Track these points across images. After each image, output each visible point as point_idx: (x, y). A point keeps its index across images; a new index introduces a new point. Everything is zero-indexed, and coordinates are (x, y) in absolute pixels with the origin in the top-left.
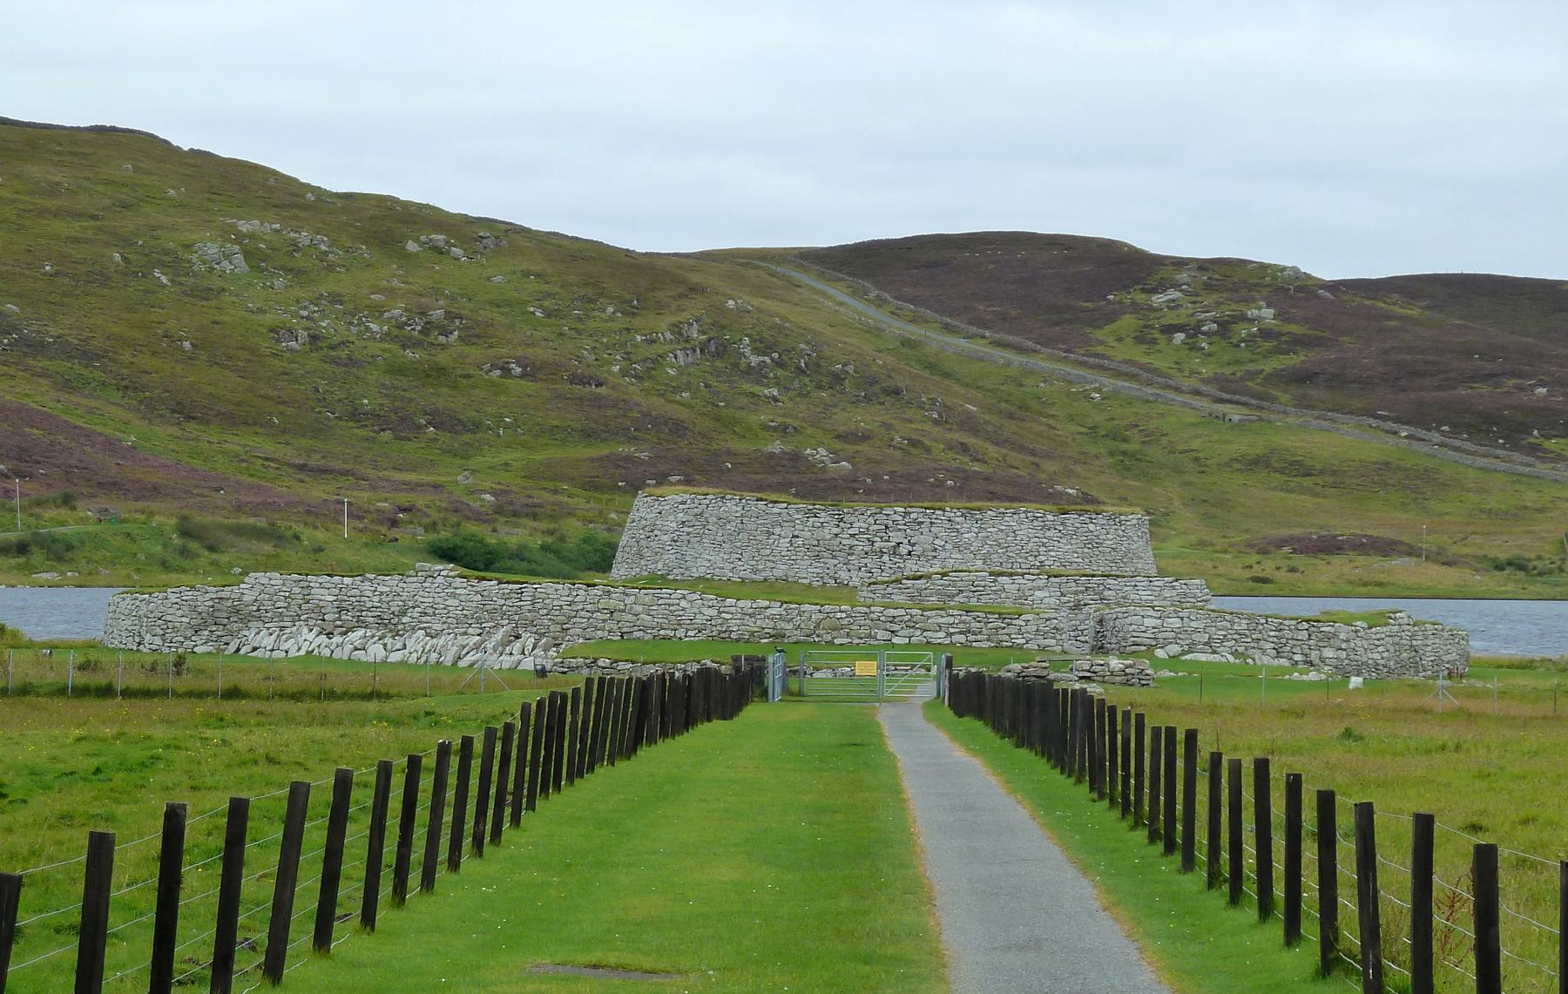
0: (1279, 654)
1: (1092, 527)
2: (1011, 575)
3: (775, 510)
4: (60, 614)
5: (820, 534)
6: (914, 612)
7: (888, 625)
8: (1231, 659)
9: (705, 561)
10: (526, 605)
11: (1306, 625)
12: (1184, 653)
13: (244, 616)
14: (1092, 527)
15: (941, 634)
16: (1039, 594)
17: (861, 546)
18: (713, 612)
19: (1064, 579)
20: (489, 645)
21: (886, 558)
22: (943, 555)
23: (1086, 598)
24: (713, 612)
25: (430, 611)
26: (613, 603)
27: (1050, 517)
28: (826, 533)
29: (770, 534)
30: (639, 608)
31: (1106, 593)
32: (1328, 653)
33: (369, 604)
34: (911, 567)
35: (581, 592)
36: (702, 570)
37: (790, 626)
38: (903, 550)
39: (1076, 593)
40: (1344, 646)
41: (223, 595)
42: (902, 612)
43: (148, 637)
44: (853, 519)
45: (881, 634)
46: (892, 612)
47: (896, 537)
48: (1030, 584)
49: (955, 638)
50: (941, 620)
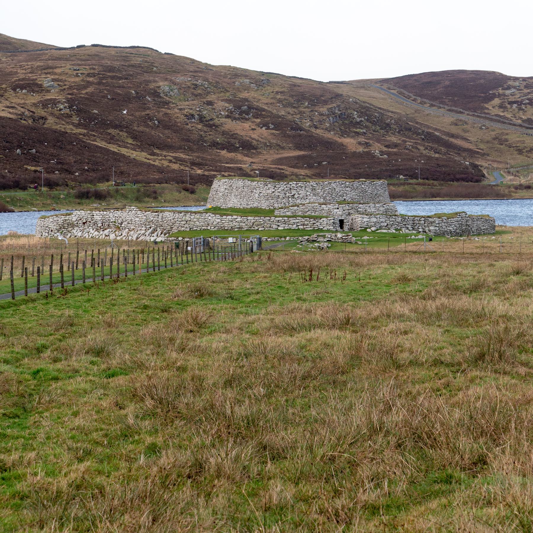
0: (413, 229)
1: (363, 186)
3: (254, 184)
4: (25, 226)
5: (268, 191)
6: (285, 218)
7: (277, 223)
8: (394, 231)
9: (234, 202)
10: (160, 220)
11: (423, 219)
12: (377, 230)
13: (73, 225)
14: (363, 186)
15: (295, 226)
18: (219, 220)
19: (344, 205)
20: (147, 234)
21: (290, 199)
22: (310, 197)
24: (219, 220)
25: (130, 222)
26: (187, 218)
27: (348, 183)
30: (195, 220)
31: (359, 209)
32: (432, 228)
33: (112, 221)
34: (299, 201)
35: (177, 215)
36: (231, 205)
37: (244, 224)
38: (296, 196)
39: (348, 210)
40: (437, 225)
41: (66, 218)
42: (281, 219)
43: (44, 233)
45: (275, 227)
46: (277, 219)
47: (293, 192)
49: (300, 227)
50: (295, 221)
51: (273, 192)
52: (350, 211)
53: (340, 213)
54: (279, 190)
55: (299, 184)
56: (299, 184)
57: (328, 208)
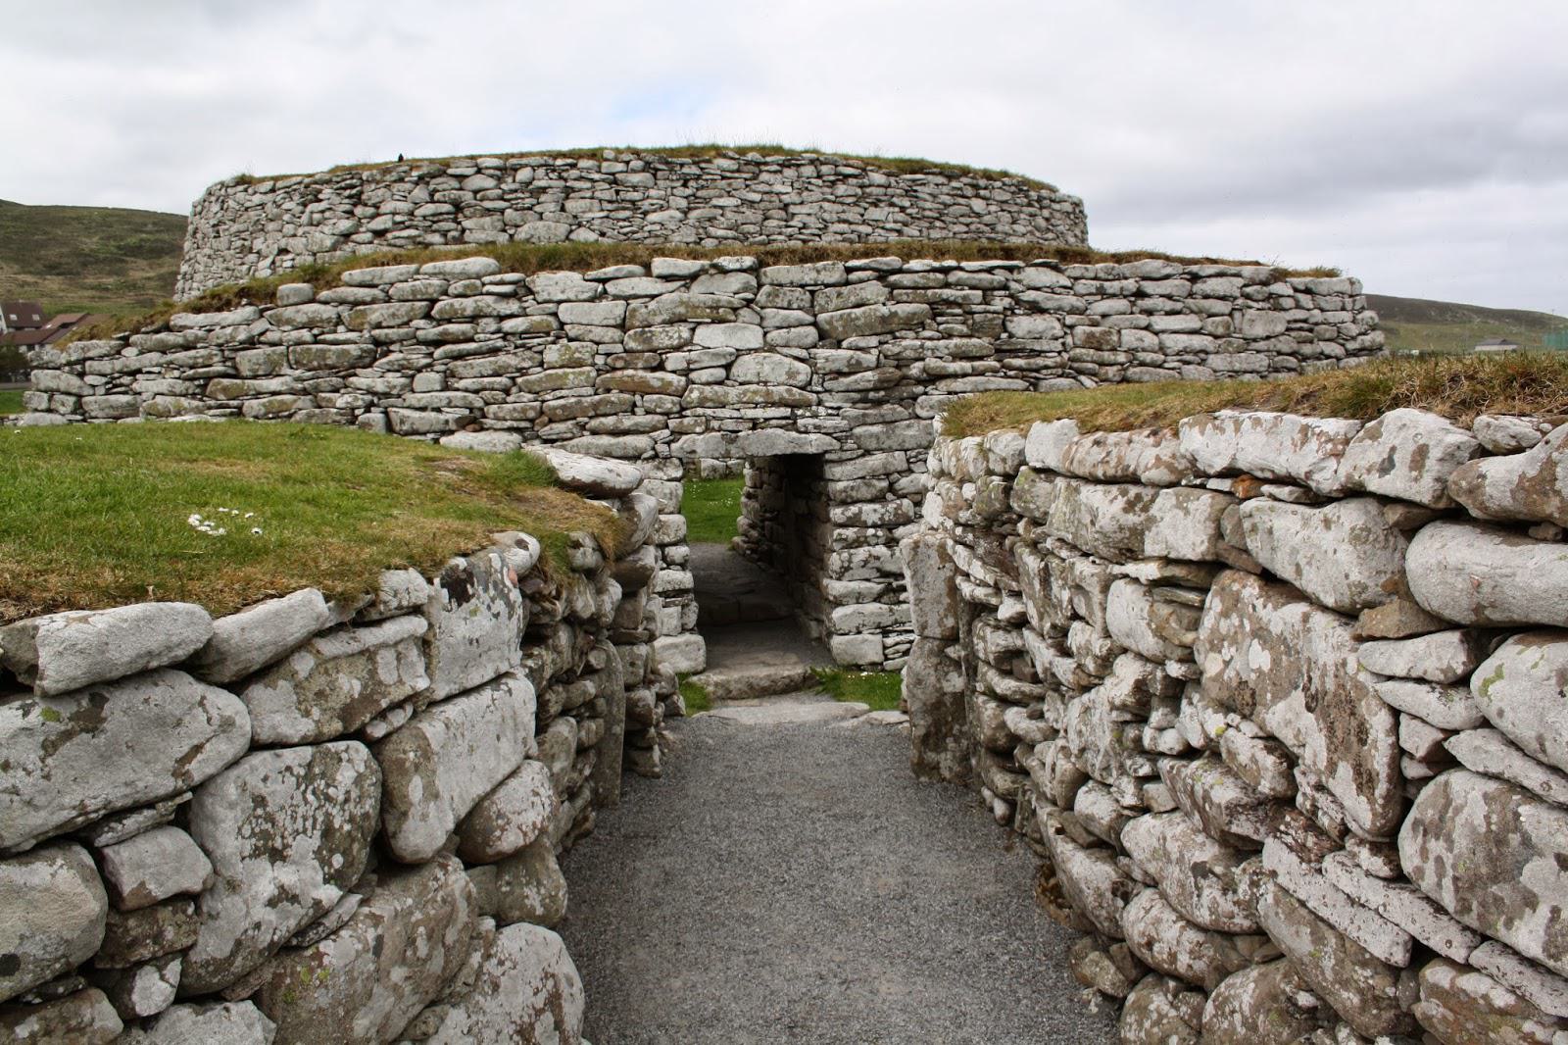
1: (978, 205)
2: (580, 260)
14: (978, 205)
16: (713, 337)
19: (833, 272)
23: (932, 349)
27: (878, 178)
31: (1023, 325)
39: (887, 328)
48: (672, 297)
51: (346, 236)
52: (909, 343)
53: (779, 370)
54: (379, 224)
55: (523, 175)
56: (523, 175)
57: (613, 310)
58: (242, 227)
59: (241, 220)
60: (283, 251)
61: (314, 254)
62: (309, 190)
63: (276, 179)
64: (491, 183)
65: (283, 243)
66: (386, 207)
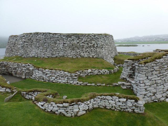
3: (56, 36)
5: (72, 42)
17: (86, 46)
21: (92, 48)
28: (75, 42)
29: (56, 43)
38: (96, 46)
44: (82, 37)
56: (96, 36)
58: (54, 40)
59: (53, 39)
60: (65, 44)
61: (73, 44)
62: (69, 36)
63: (61, 34)
64: (93, 37)
65: (65, 42)
66: (83, 39)
